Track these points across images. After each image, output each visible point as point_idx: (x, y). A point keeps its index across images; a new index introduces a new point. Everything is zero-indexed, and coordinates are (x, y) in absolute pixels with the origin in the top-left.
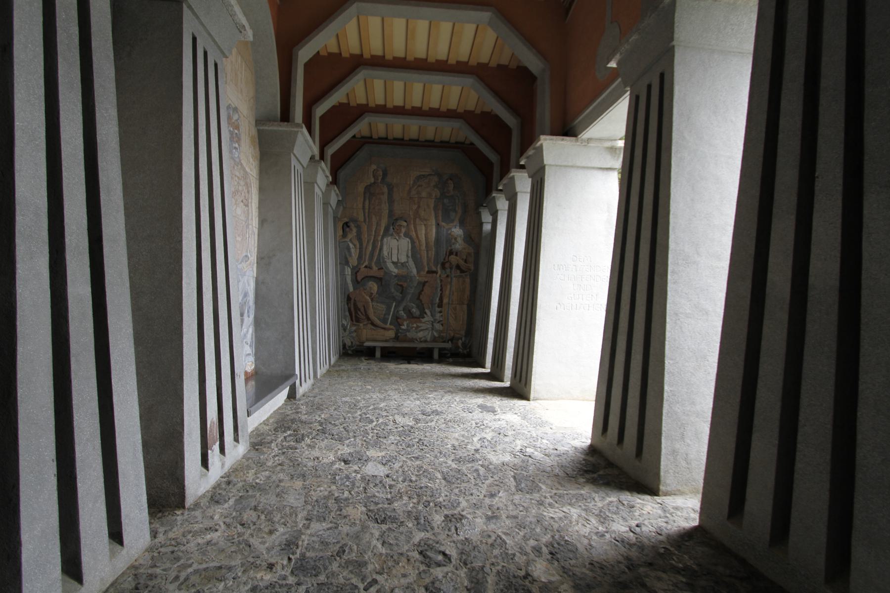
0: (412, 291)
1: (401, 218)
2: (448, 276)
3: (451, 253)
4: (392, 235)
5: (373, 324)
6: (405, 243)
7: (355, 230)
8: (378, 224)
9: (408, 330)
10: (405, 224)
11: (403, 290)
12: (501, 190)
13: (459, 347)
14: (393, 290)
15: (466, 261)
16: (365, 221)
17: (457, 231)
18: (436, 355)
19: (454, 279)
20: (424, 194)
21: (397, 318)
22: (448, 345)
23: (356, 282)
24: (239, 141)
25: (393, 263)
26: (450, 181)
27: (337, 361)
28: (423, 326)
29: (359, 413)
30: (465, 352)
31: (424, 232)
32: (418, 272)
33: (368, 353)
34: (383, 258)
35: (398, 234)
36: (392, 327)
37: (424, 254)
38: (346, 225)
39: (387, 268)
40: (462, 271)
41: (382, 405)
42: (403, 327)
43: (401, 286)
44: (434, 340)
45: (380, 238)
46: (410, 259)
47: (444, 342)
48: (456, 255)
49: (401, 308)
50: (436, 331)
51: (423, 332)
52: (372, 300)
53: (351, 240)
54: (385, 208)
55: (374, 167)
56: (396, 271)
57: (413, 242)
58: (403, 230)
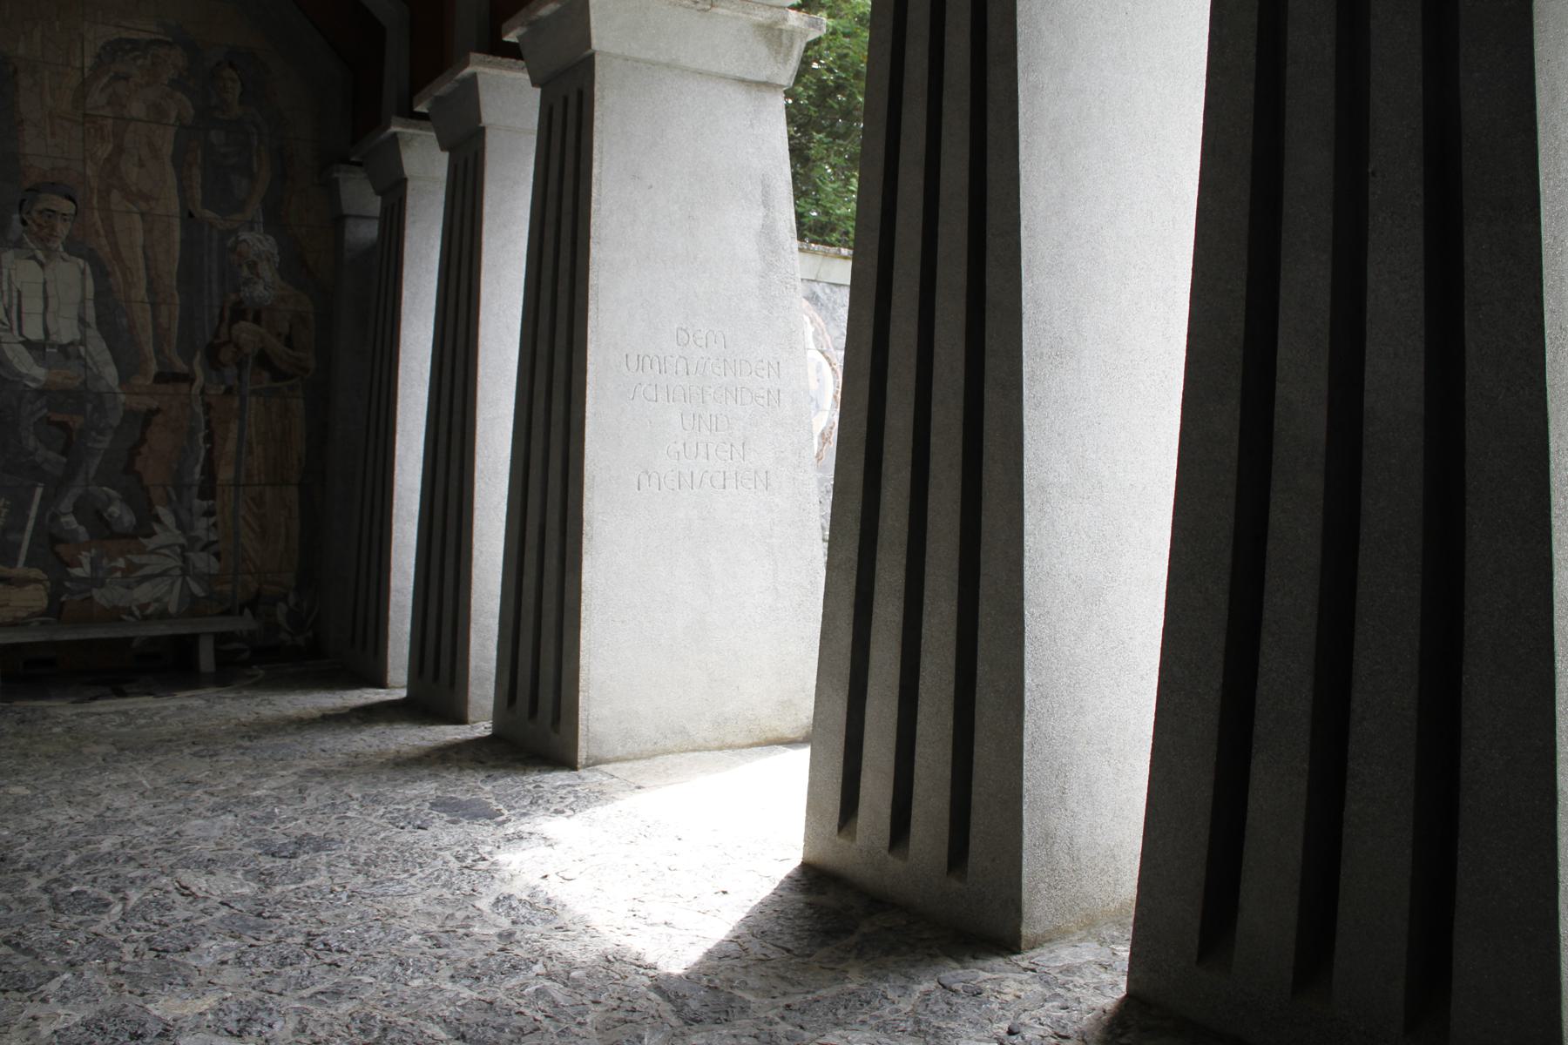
0: (105, 443)
3: (238, 313)
4: (19, 244)
6: (70, 279)
9: (96, 581)
10: (67, 207)
12: (423, 117)
14: (31, 442)
15: (289, 342)
17: (259, 243)
20: (137, 109)
21: (55, 540)
22: (244, 624)
25: (28, 344)
29: (35, 883)
31: (139, 238)
32: (124, 379)
36: (34, 573)
40: (278, 375)
41: (107, 844)
42: (77, 572)
43: (63, 426)
44: (193, 608)
46: (93, 333)
47: (227, 613)
48: (257, 320)
49: (66, 504)
56: (40, 373)
57: (101, 273)
58: (63, 229)
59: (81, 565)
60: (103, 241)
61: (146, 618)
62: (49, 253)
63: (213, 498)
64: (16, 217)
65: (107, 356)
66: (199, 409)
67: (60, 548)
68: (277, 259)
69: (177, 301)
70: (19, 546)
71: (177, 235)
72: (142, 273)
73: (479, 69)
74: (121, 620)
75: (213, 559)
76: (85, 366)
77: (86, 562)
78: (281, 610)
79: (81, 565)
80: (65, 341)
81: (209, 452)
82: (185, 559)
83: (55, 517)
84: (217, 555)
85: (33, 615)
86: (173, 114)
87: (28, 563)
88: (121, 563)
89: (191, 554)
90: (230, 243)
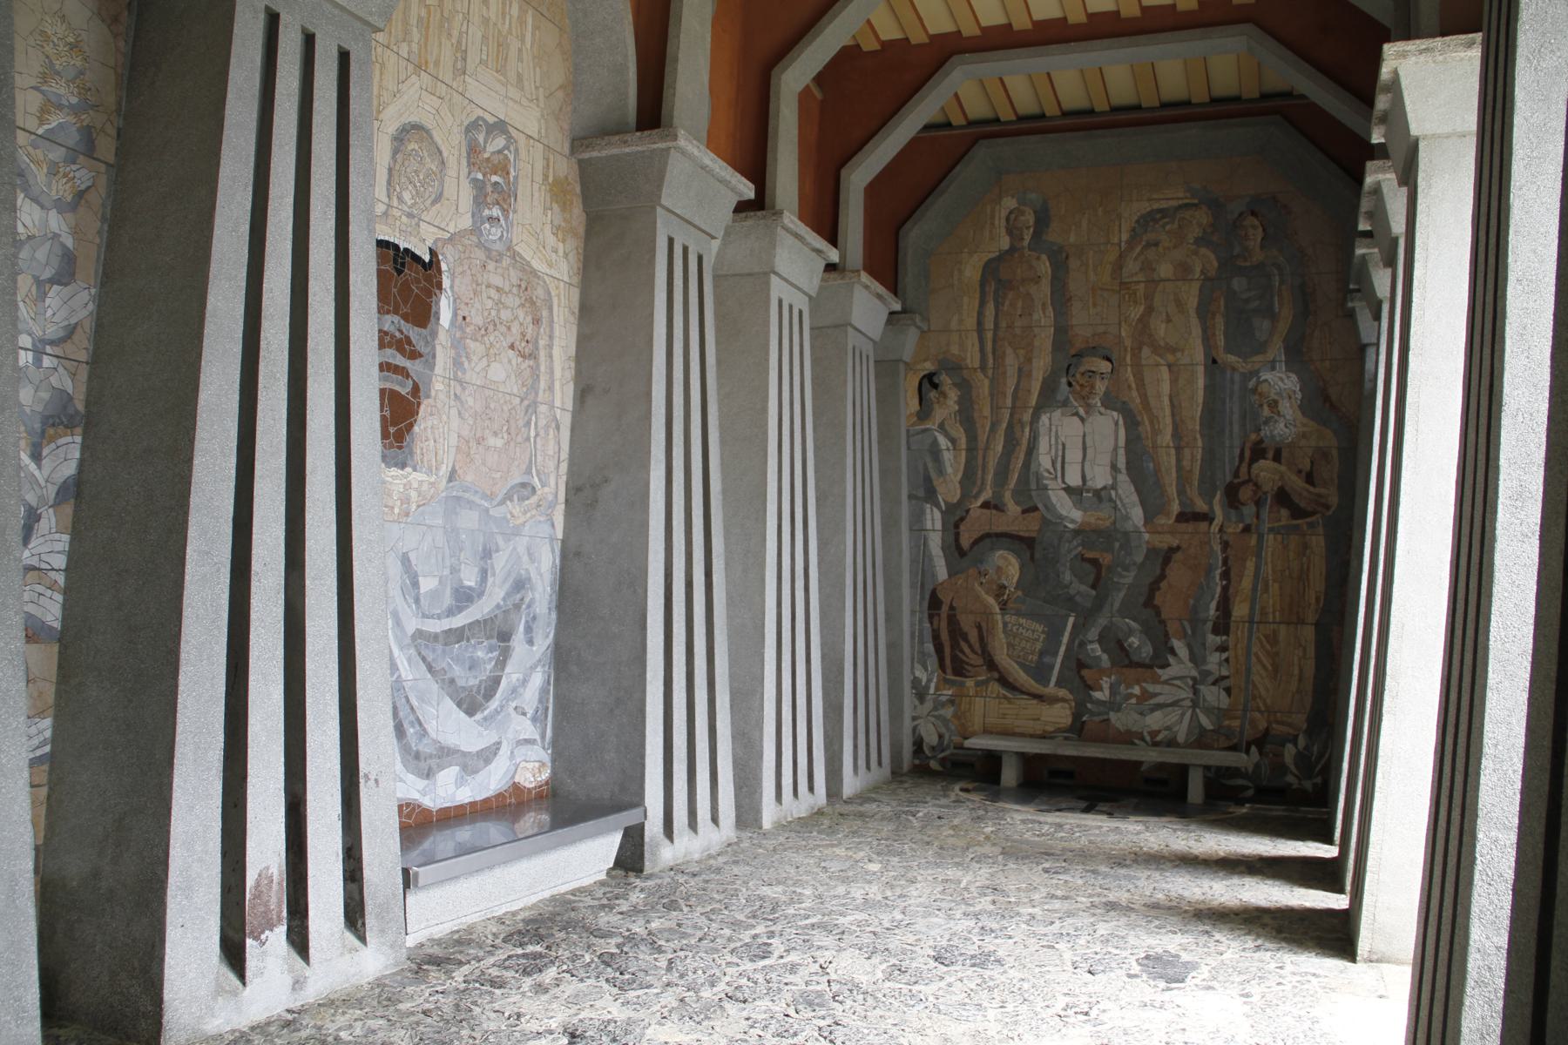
0: (1129, 578)
1: (1093, 351)
2: (1247, 529)
3: (1258, 452)
4: (1065, 403)
5: (1004, 681)
6: (1106, 429)
7: (953, 395)
8: (1023, 373)
9: (1113, 705)
10: (1105, 366)
11: (1098, 576)
13: (1281, 769)
14: (1067, 577)
15: (1310, 478)
16: (983, 368)
17: (1282, 382)
18: (1196, 791)
19: (1270, 539)
21: (1081, 665)
23: (957, 551)
24: (505, 197)
25: (1069, 490)
26: (1252, 221)
27: (876, 789)
28: (1166, 694)
30: (1308, 785)
31: (1166, 387)
32: (1148, 519)
33: (974, 773)
34: (1039, 478)
35: (1085, 399)
36: (1063, 693)
37: (1168, 460)
38: (930, 381)
39: (1049, 507)
40: (1297, 513)
42: (1097, 695)
43: (1094, 562)
44: (1201, 740)
45: (1027, 417)
46: (1123, 478)
47: (1234, 748)
48: (1277, 458)
49: (1093, 633)
50: (1208, 711)
51: (1163, 712)
52: (1004, 606)
53: (942, 426)
54: (1044, 321)
55: (1010, 203)
56: (1077, 515)
57: (1132, 423)
58: (1101, 387)
59: (1101, 689)
60: (1135, 394)
61: (1156, 744)
62: (1089, 408)
63: (1227, 633)
64: (1064, 380)
65: (1135, 498)
66: (1217, 548)
67: (1085, 672)
68: (1299, 396)
69: (1200, 443)
70: (1052, 667)
71: (1201, 382)
72: (1168, 420)
73: (1380, 177)
74: (1133, 743)
75: (1223, 693)
76: (1115, 508)
77: (1106, 686)
78: (1289, 752)
79: (1101, 689)
80: (1099, 486)
81: (1225, 589)
82: (1196, 692)
83: (1082, 644)
84: (1228, 690)
85: (1059, 730)
86: (1198, 270)
87: (1059, 684)
88: (1136, 690)
89: (1202, 687)
90: (1251, 384)
